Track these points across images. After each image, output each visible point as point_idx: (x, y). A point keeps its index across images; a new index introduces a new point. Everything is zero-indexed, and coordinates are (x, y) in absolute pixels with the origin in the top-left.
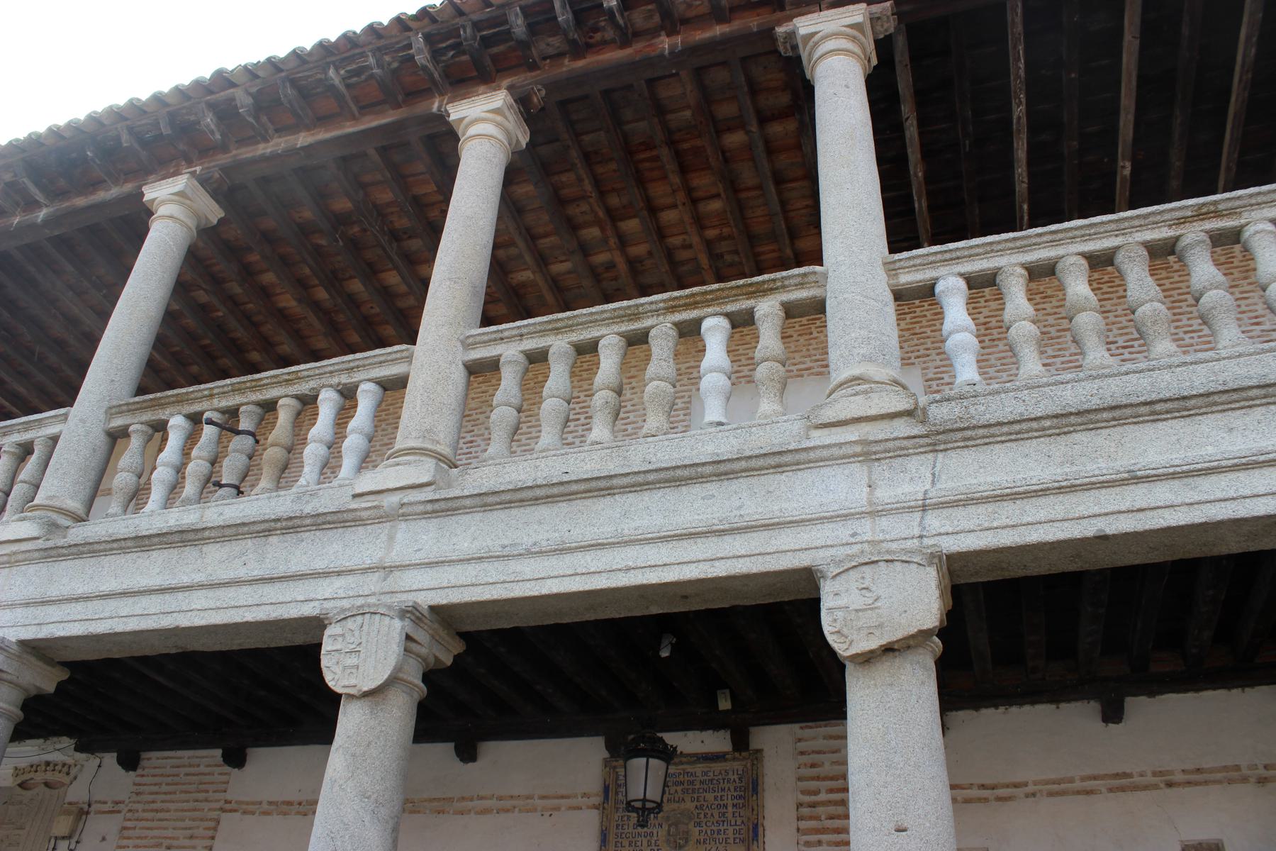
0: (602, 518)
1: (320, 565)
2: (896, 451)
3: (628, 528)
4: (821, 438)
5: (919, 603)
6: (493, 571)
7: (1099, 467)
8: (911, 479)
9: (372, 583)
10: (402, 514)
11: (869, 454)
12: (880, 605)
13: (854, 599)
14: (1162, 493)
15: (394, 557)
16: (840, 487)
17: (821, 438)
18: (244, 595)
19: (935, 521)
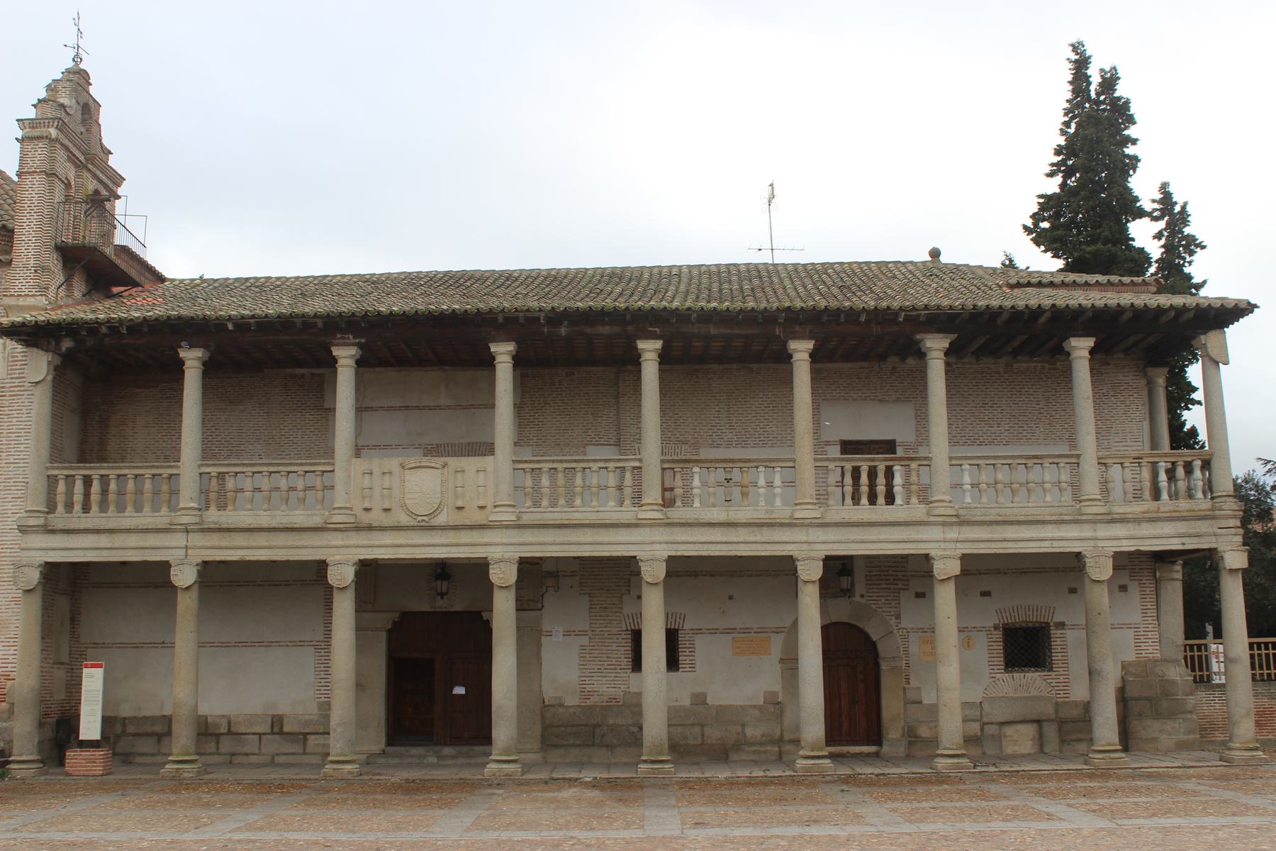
0: (872, 534)
1: (786, 539)
2: (952, 524)
3: (882, 537)
4: (933, 519)
5: (955, 568)
6: (843, 546)
7: (996, 536)
8: (953, 534)
9: (805, 547)
10: (811, 525)
11: (944, 524)
12: (946, 567)
13: (941, 566)
14: (1010, 545)
15: (811, 538)
16: (936, 533)
17: (933, 519)
18: (759, 547)
19: (959, 545)
